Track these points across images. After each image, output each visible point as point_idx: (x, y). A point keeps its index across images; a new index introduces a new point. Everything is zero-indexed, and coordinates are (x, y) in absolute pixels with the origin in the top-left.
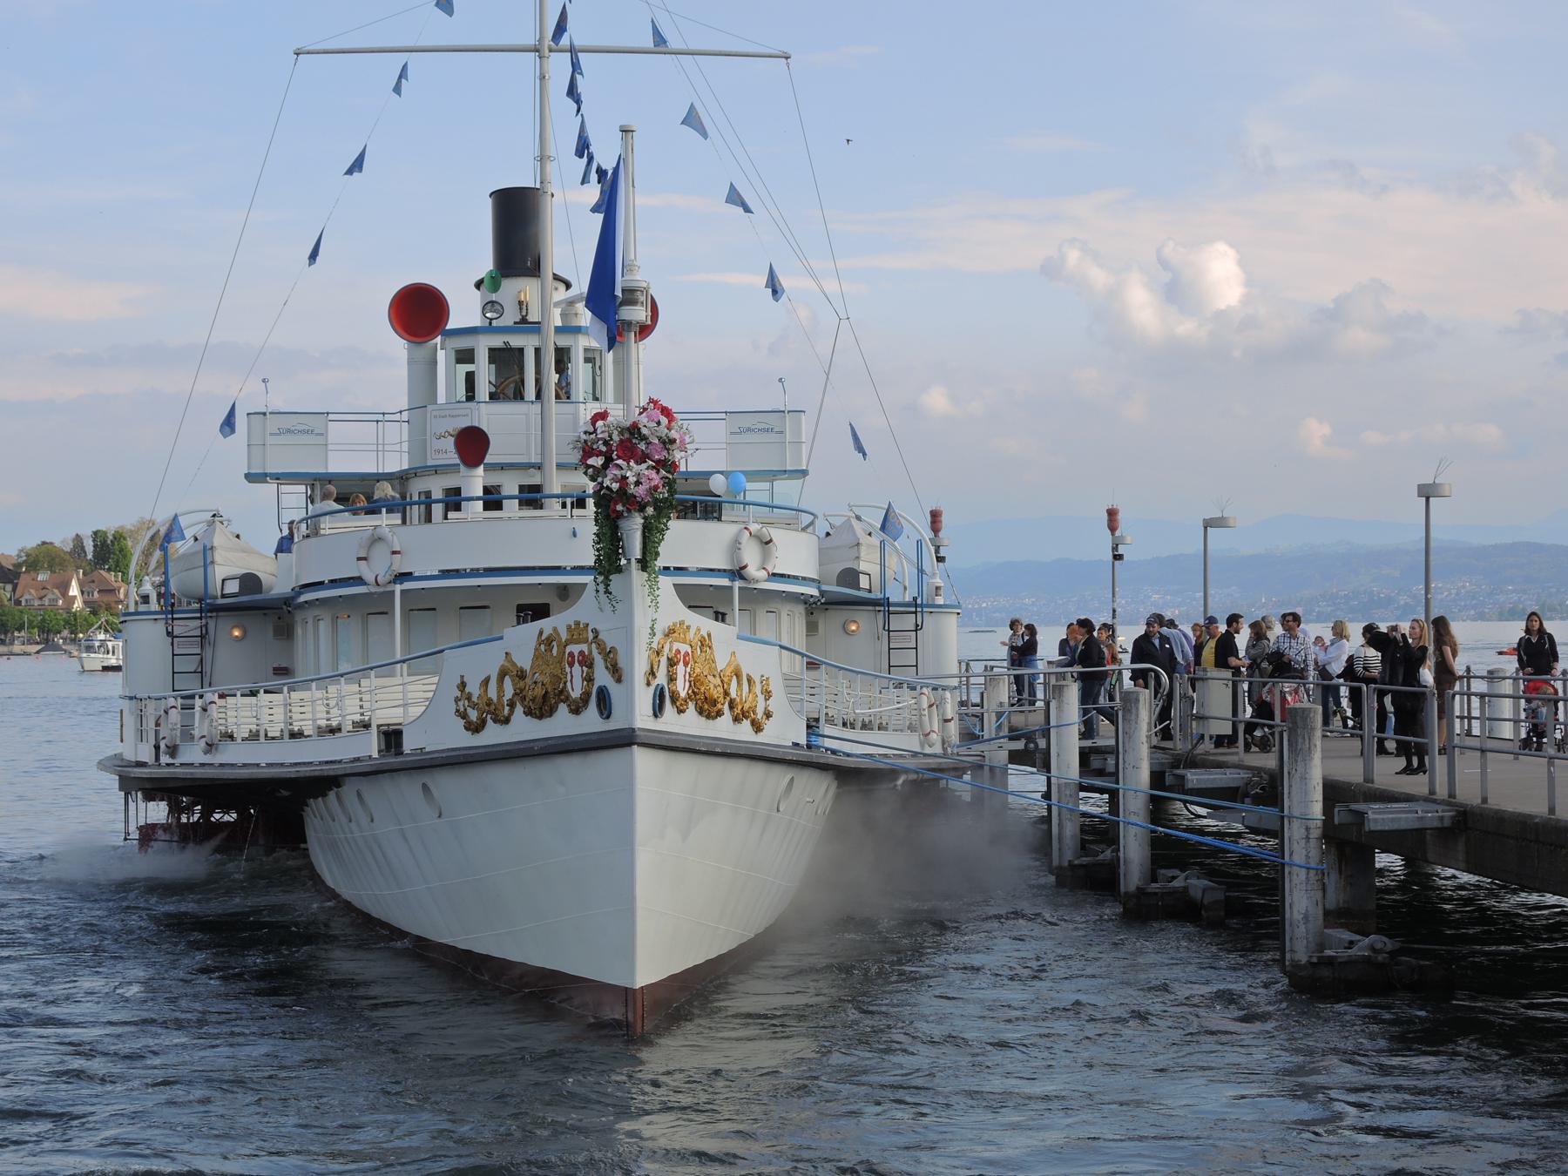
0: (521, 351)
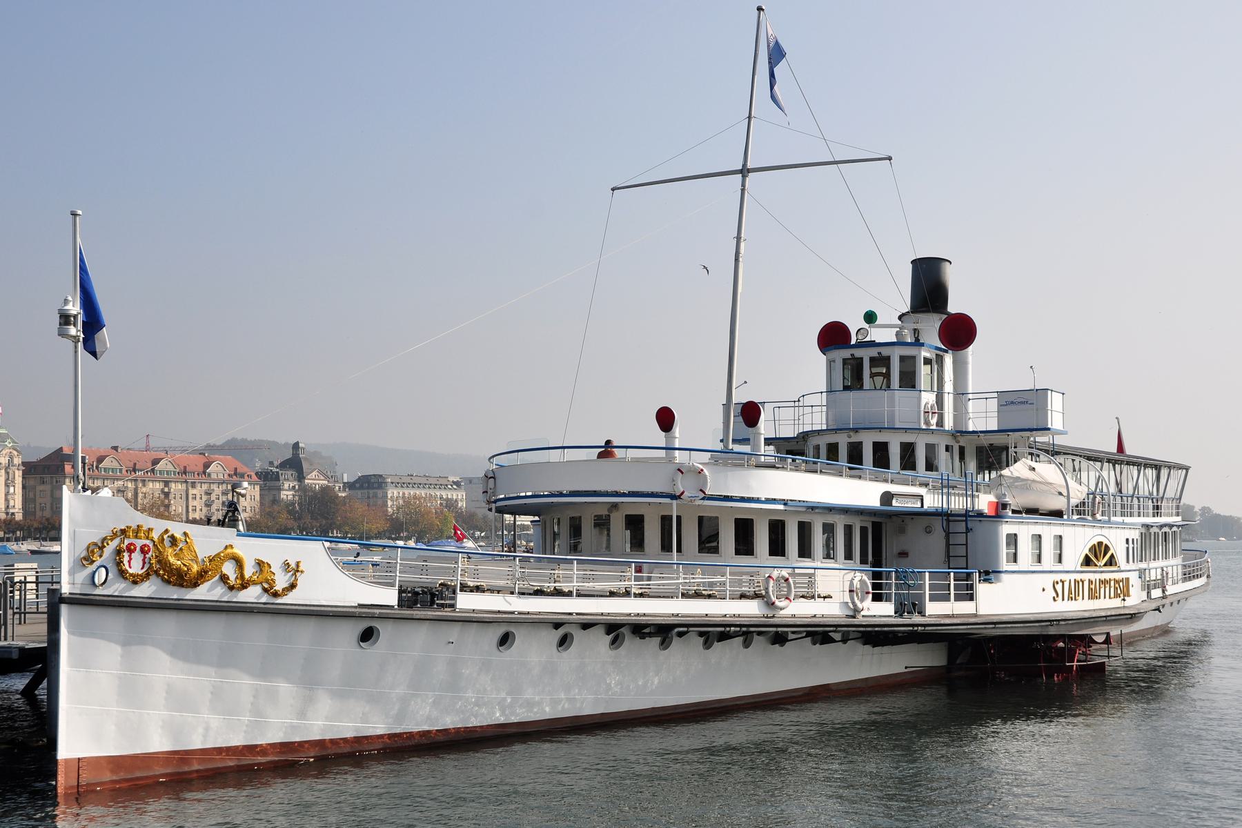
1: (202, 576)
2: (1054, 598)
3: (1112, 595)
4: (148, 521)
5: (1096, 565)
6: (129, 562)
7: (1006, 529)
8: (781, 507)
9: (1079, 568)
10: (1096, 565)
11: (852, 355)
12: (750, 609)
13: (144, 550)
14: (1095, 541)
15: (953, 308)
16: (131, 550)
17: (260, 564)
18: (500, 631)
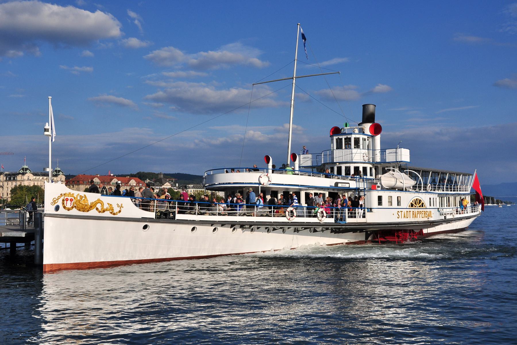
0: (341, 139)
2: (398, 217)
3: (423, 216)
5: (415, 207)
6: (66, 204)
9: (408, 207)
10: (415, 207)
11: (339, 138)
13: (71, 200)
14: (415, 198)
15: (376, 122)
16: (67, 200)
17: (108, 204)
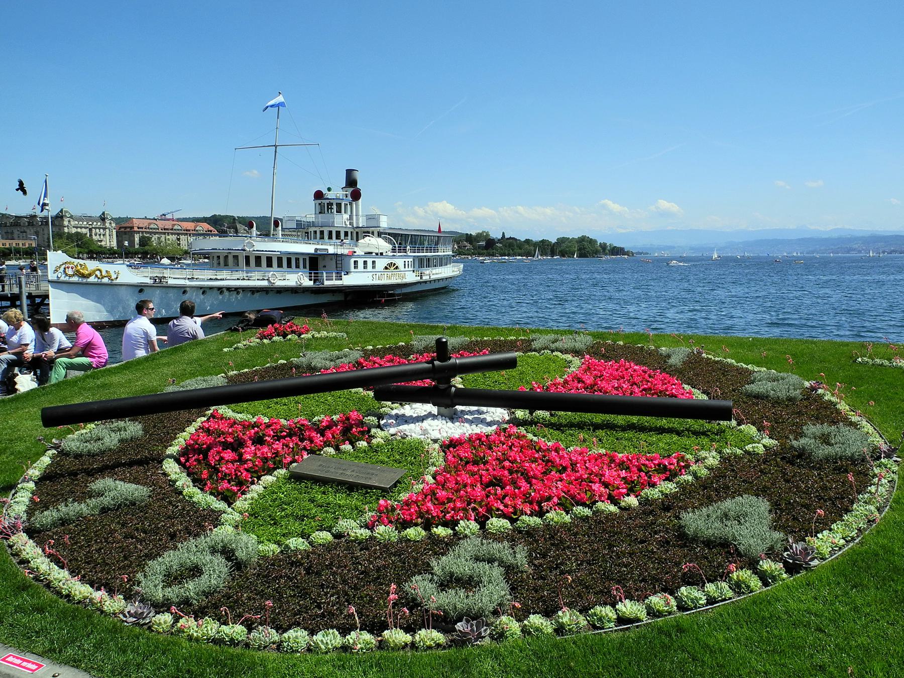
1: (90, 275)
4: (73, 260)
7: (352, 260)
8: (279, 253)
9: (382, 270)
12: (265, 283)
13: (72, 268)
16: (68, 268)
17: (107, 271)
18: (183, 290)
